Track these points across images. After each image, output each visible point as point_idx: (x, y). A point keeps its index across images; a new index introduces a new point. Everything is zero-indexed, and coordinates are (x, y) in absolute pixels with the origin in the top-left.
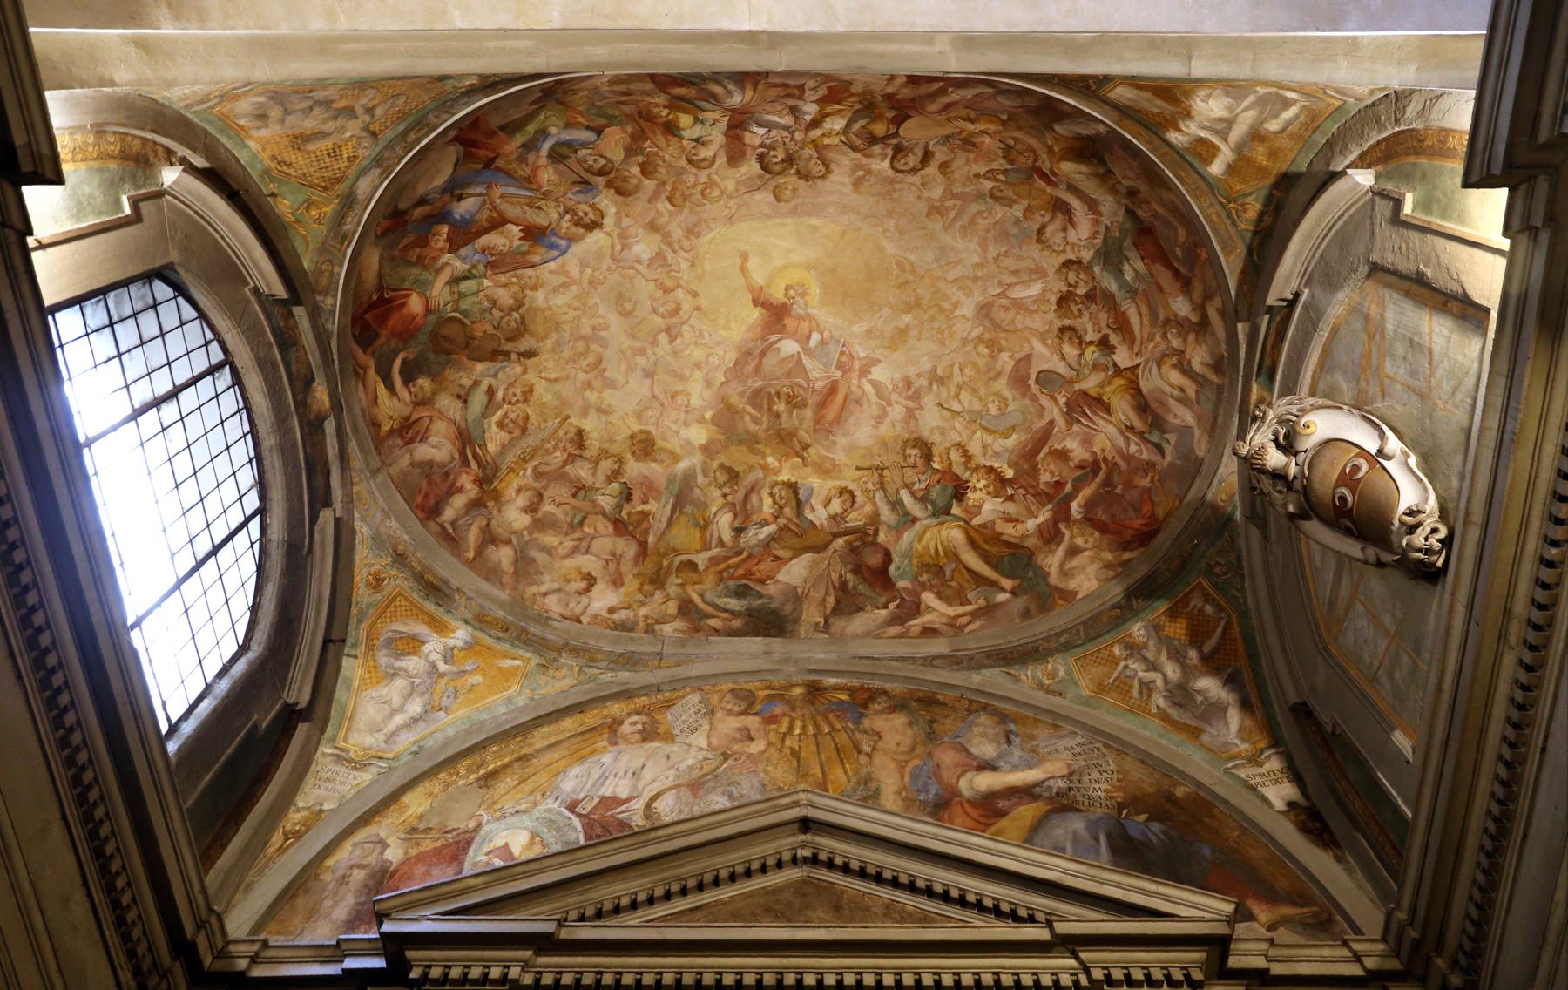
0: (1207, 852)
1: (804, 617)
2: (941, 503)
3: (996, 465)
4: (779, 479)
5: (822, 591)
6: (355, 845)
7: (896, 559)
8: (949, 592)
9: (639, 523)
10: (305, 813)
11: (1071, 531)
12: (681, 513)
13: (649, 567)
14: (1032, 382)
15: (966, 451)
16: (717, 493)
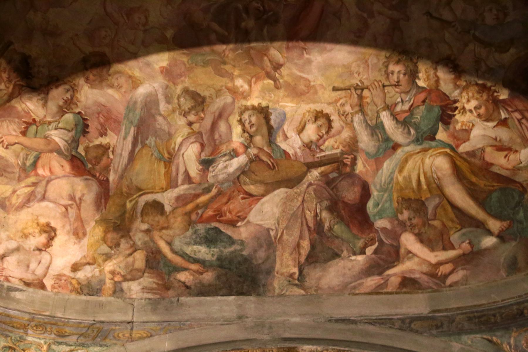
1: (278, 266)
2: (425, 127)
4: (249, 103)
5: (296, 234)
7: (375, 193)
8: (431, 234)
9: (98, 160)
12: (144, 145)
13: (112, 209)
16: (181, 121)
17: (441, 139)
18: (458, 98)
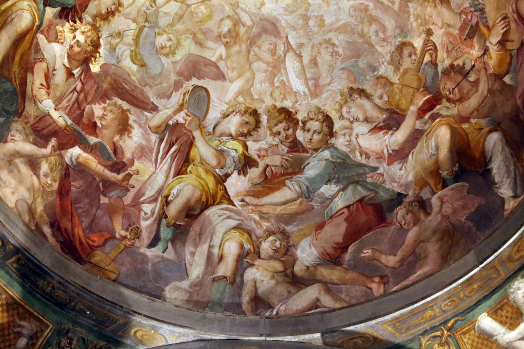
3: (102, 50)
11: (50, 155)
14: (195, 81)
15: (113, 13)
17: (46, 14)
18: (84, 22)
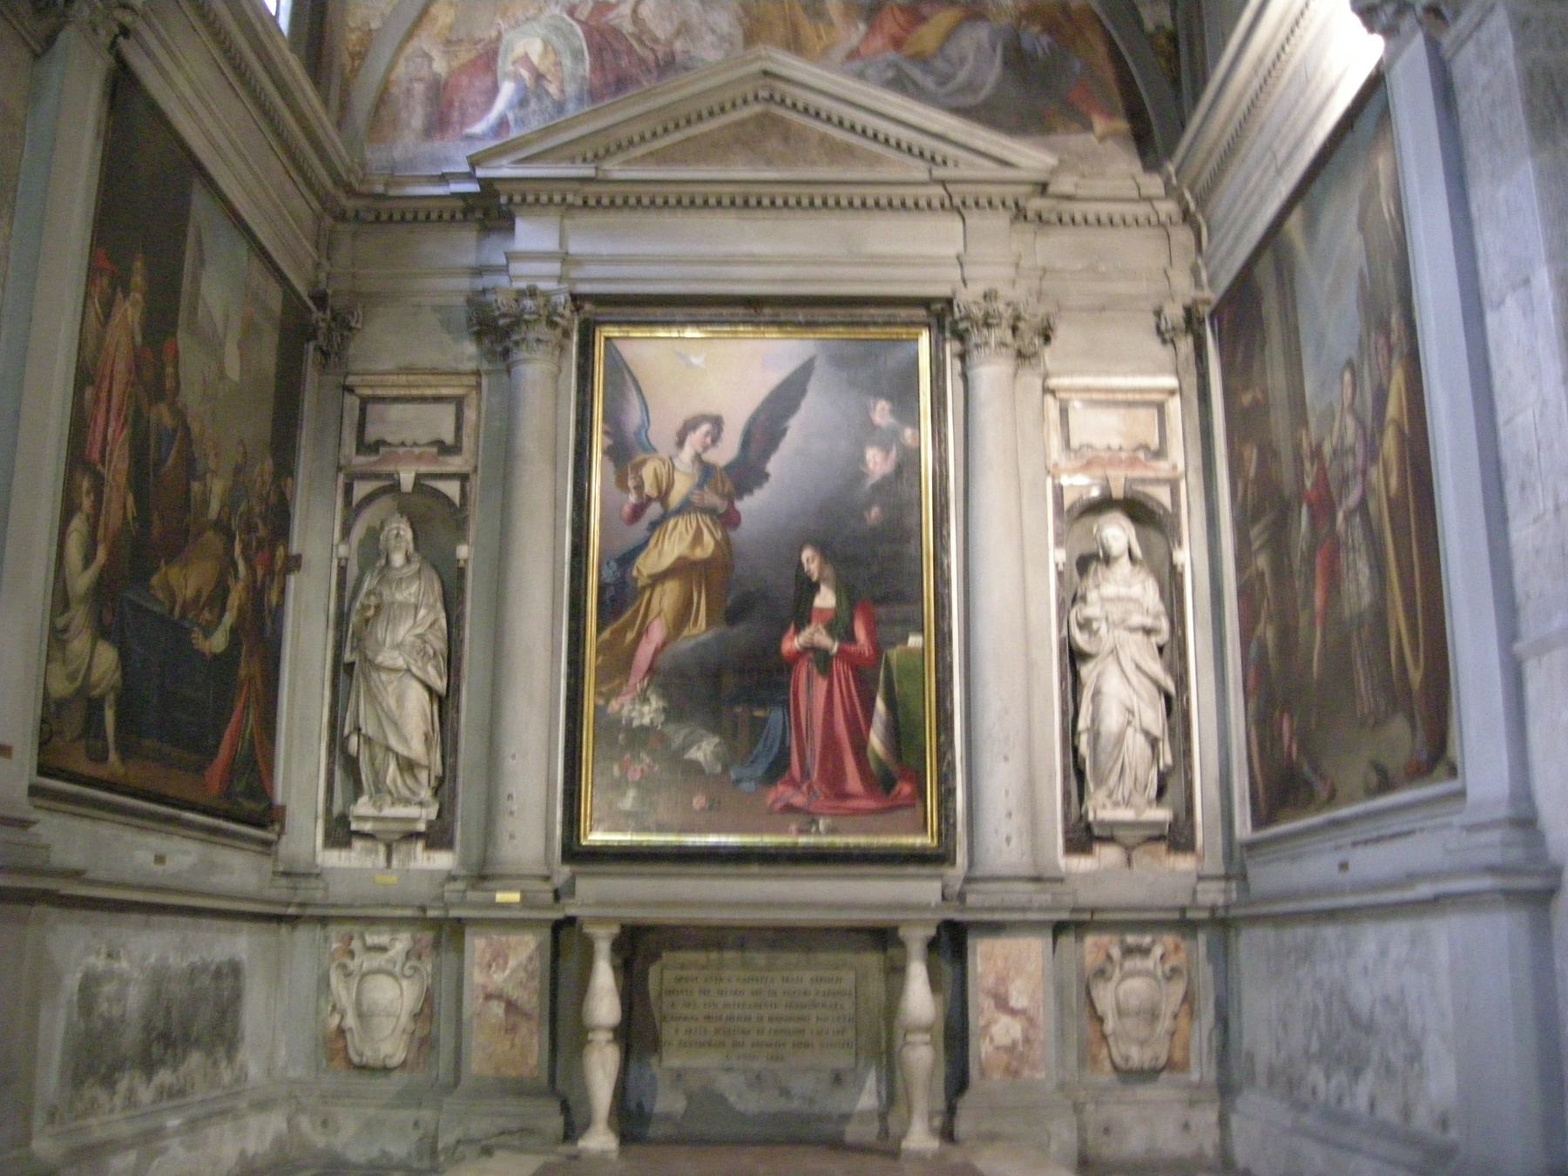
0: (1077, 66)
6: (407, 60)
10: (358, 33)
